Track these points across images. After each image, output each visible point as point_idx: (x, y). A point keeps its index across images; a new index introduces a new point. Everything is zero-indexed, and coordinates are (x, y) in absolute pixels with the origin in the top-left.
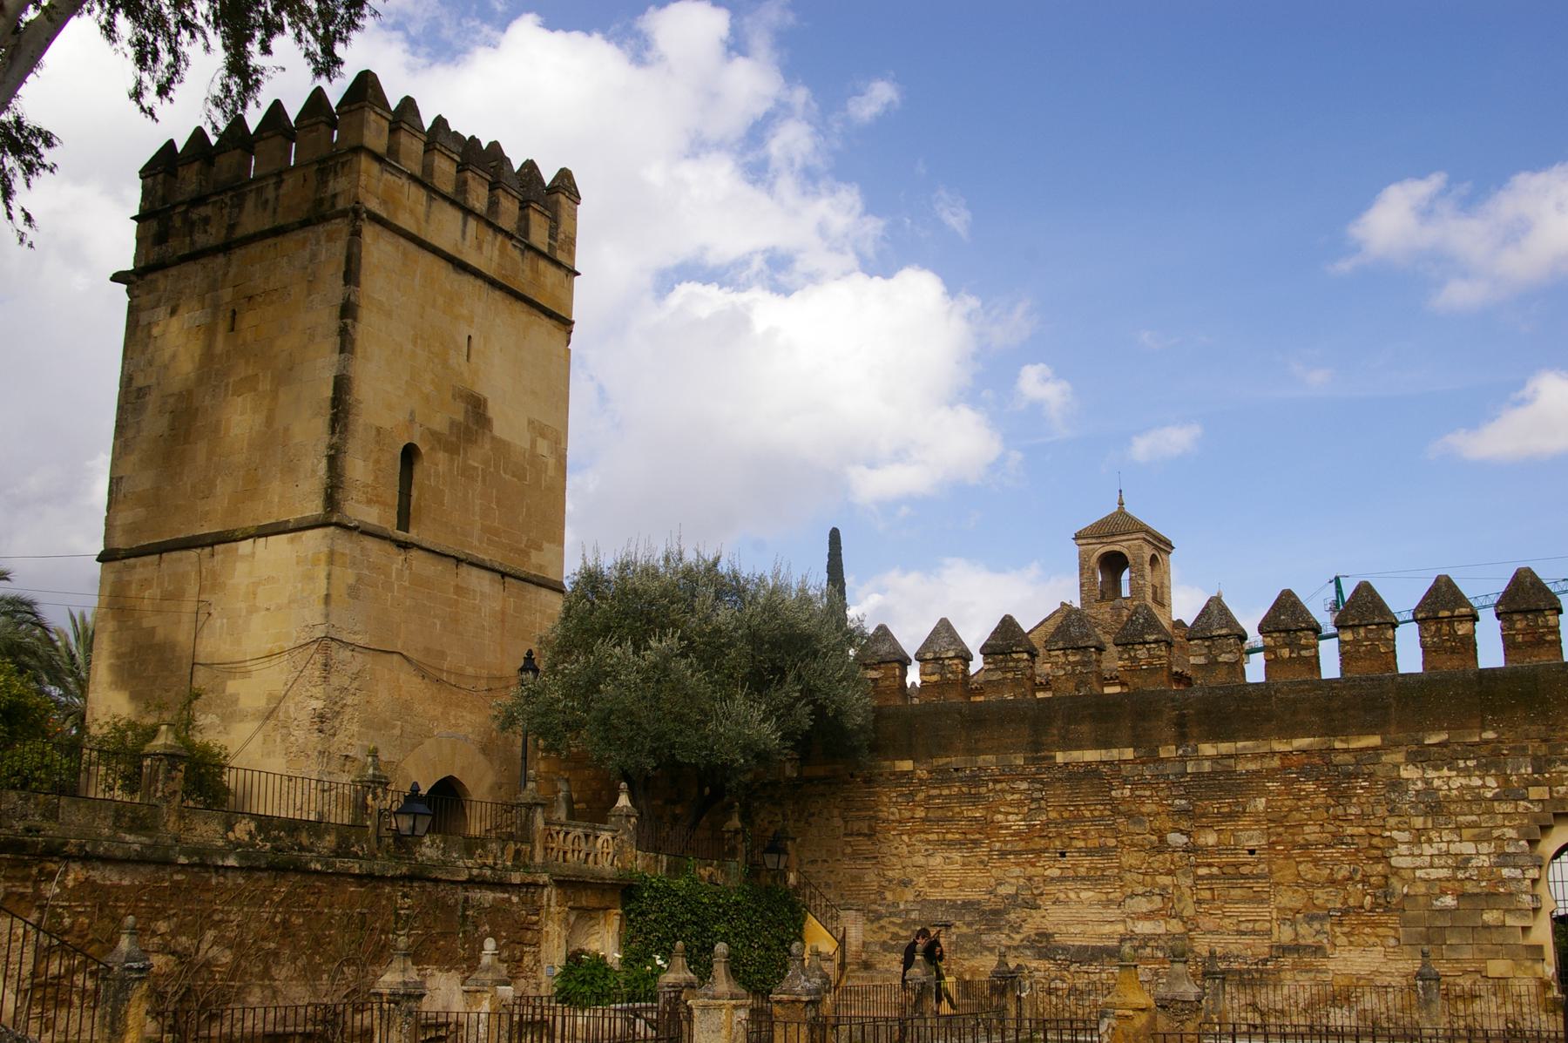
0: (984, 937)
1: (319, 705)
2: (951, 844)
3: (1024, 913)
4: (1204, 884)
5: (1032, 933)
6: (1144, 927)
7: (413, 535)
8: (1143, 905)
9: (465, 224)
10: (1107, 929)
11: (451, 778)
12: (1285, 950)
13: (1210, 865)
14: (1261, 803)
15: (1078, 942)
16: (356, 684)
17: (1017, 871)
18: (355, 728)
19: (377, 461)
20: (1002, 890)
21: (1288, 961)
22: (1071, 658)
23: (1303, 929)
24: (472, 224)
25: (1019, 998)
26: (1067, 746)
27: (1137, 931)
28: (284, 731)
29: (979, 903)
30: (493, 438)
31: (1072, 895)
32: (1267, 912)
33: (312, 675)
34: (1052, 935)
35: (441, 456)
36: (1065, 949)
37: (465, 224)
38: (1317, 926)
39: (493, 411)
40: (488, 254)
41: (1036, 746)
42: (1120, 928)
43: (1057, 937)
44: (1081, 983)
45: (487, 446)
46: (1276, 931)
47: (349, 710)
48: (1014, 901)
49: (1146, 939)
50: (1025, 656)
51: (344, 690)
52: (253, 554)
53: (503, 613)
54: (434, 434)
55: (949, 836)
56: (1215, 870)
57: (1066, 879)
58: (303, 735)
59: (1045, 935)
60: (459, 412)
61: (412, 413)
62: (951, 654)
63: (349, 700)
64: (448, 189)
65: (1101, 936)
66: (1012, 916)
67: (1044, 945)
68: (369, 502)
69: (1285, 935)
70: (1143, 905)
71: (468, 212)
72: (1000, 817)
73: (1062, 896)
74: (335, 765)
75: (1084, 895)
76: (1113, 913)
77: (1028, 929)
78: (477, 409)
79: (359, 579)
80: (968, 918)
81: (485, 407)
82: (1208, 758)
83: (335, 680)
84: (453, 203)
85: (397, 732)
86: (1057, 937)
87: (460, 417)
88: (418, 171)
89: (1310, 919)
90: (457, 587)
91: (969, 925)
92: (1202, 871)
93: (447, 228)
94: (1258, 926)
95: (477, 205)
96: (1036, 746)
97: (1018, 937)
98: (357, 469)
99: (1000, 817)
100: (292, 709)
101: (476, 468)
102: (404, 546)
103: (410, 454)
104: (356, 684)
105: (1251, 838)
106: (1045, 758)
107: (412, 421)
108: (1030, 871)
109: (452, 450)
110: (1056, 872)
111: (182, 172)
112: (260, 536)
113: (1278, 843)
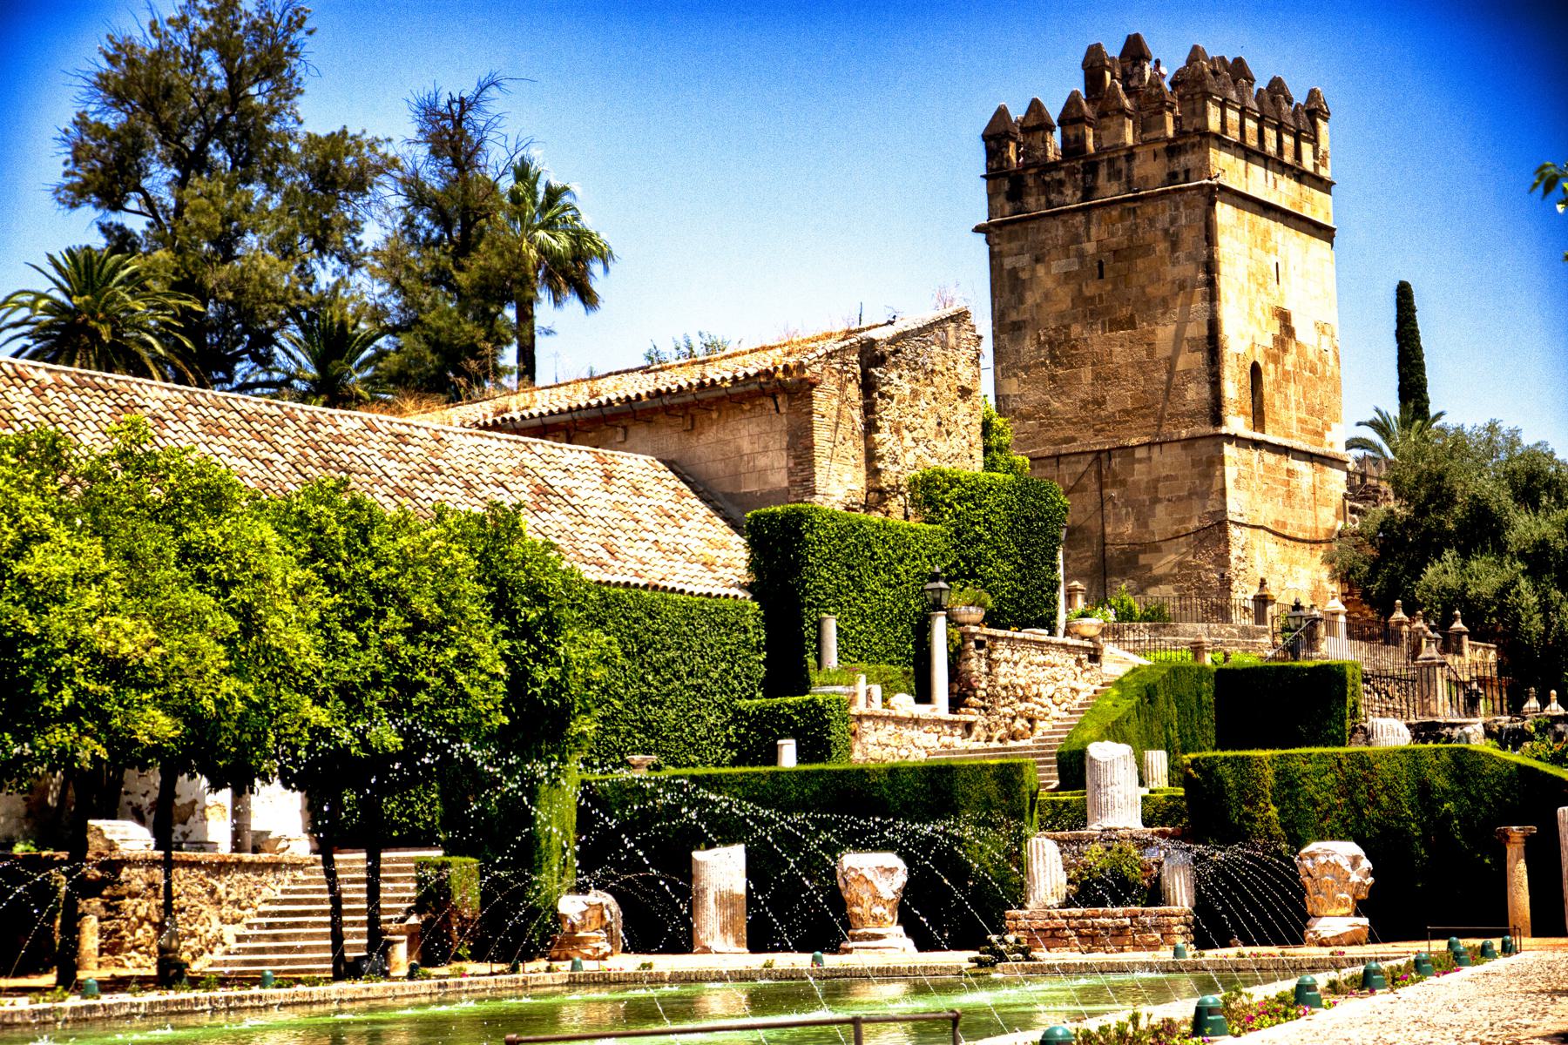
40: (1283, 192)
52: (1150, 458)
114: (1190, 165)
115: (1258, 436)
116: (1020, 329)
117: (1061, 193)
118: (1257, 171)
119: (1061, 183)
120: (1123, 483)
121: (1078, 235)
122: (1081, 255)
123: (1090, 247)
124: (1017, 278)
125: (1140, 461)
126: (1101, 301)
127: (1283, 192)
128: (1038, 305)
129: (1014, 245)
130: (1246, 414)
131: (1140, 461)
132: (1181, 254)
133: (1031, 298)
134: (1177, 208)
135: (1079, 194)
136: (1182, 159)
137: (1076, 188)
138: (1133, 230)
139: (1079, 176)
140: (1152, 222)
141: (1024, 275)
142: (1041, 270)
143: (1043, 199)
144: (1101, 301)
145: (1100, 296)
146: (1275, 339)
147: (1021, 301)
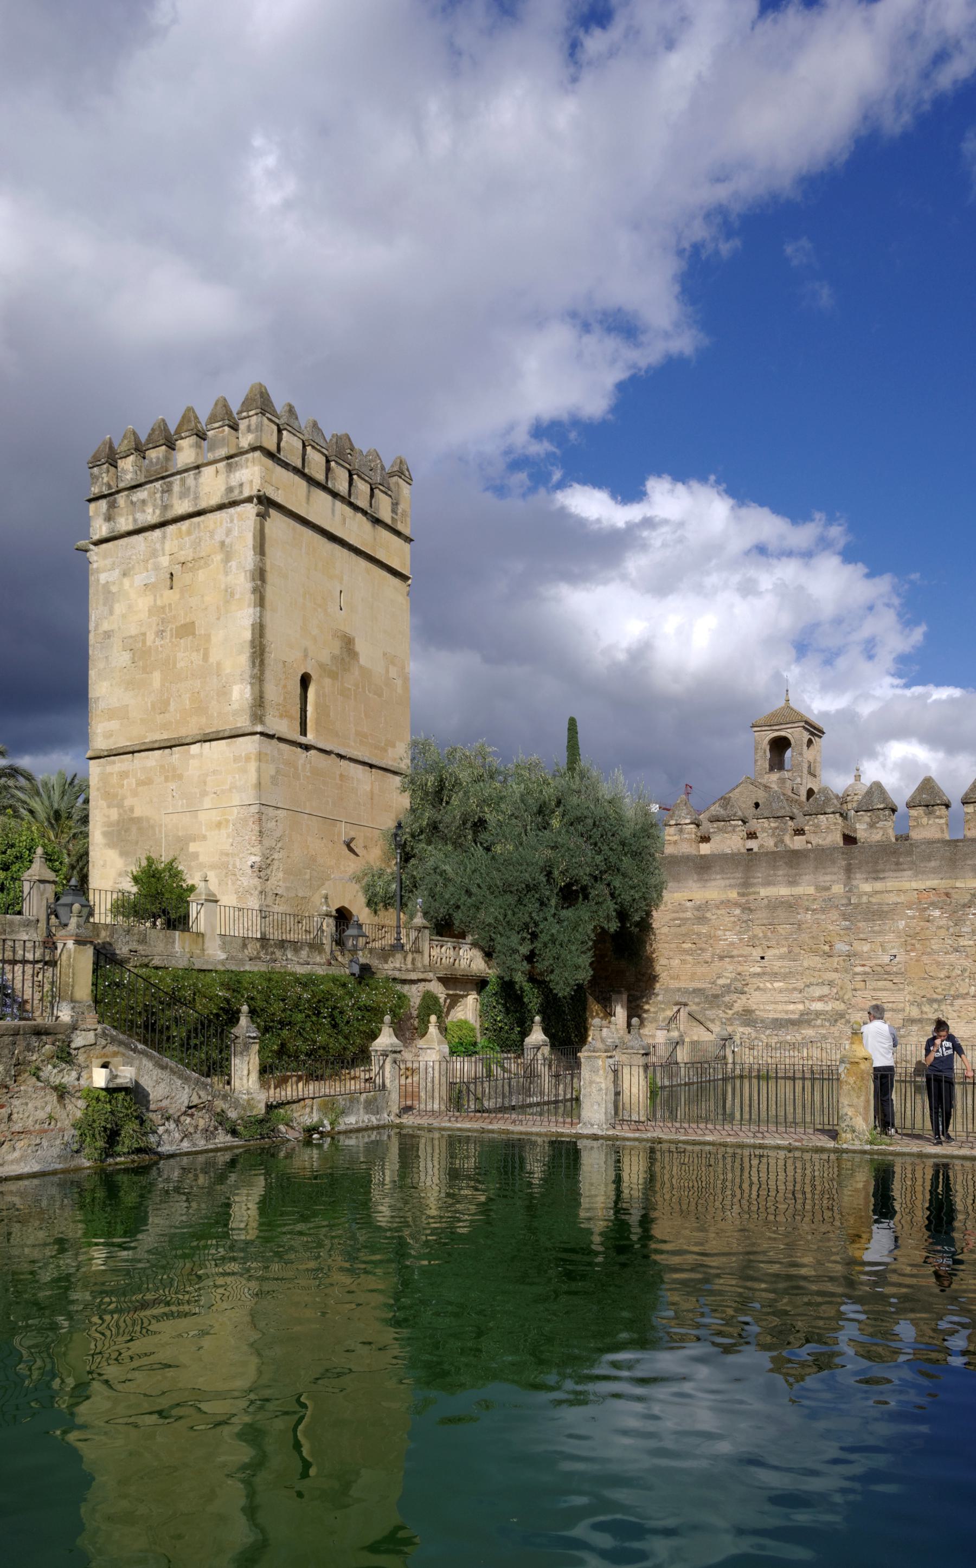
0: (707, 1012)
1: (257, 859)
2: (686, 951)
3: (734, 996)
4: (859, 978)
5: (740, 1009)
6: (818, 1006)
7: (310, 738)
8: (817, 992)
9: (334, 505)
10: (792, 1007)
11: (343, 907)
12: (913, 1021)
13: (863, 965)
14: (902, 924)
15: (772, 1015)
16: (279, 845)
17: (730, 968)
18: (281, 875)
19: (285, 686)
20: (721, 982)
21: (915, 1028)
22: (773, 825)
23: (926, 1008)
24: (338, 504)
25: (733, 1052)
26: (768, 883)
27: (812, 1008)
28: (233, 877)
29: (704, 989)
30: (361, 667)
31: (769, 985)
32: (899, 997)
33: (250, 839)
34: (753, 1011)
35: (327, 681)
36: (762, 1021)
37: (334, 505)
38: (935, 1006)
39: (360, 646)
41: (746, 884)
42: (801, 1007)
43: (757, 1013)
44: (773, 1041)
45: (357, 673)
46: (907, 1009)
47: (276, 862)
48: (727, 989)
49: (818, 1014)
50: (740, 823)
51: (272, 849)
53: (372, 792)
54: (322, 666)
55: (684, 946)
56: (867, 969)
57: (764, 974)
58: (249, 880)
59: (748, 1011)
60: (336, 647)
61: (306, 650)
62: (688, 821)
63: (276, 856)
64: (321, 477)
65: (787, 1012)
66: (727, 999)
67: (747, 1017)
68: (281, 716)
69: (915, 1013)
70: (817, 992)
71: (335, 495)
72: (720, 933)
73: (762, 985)
74: (270, 900)
75: (776, 985)
76: (796, 995)
77: (738, 1007)
78: (348, 643)
79: (278, 771)
80: (697, 1000)
81: (354, 644)
82: (866, 893)
83: (268, 843)
84: (325, 488)
85: (307, 877)
86: (757, 1013)
87: (337, 652)
88: (298, 464)
89: (931, 1001)
90: (341, 775)
91: (698, 1004)
92: (859, 969)
93: (321, 508)
94: (894, 1006)
95: (341, 488)
96: (746, 884)
97: (730, 1012)
98: (272, 693)
99: (720, 933)
100: (238, 863)
101: (349, 689)
102: (307, 748)
103: (305, 681)
104: (279, 845)
105: (893, 948)
106: (754, 893)
107: (306, 656)
108: (740, 969)
109: (333, 676)
110: (759, 970)
111: (121, 463)
112: (205, 741)
113: (912, 950)
114: (244, 479)
115: (303, 740)
116: (109, 637)
117: (144, 511)
118: (322, 498)
119: (144, 502)
120: (180, 777)
121: (155, 550)
122: (157, 568)
123: (164, 561)
124: (109, 592)
125: (193, 757)
126: (171, 610)
127: (355, 529)
128: (124, 616)
129: (108, 562)
130: (291, 718)
131: (193, 757)
132: (233, 564)
133: (119, 608)
134: (232, 521)
135: (158, 512)
136: (238, 474)
137: (155, 506)
138: (197, 544)
139: (158, 495)
140: (212, 533)
141: (114, 589)
142: (126, 582)
143: (131, 518)
144: (171, 610)
145: (170, 604)
146: (334, 658)
147: (111, 612)
